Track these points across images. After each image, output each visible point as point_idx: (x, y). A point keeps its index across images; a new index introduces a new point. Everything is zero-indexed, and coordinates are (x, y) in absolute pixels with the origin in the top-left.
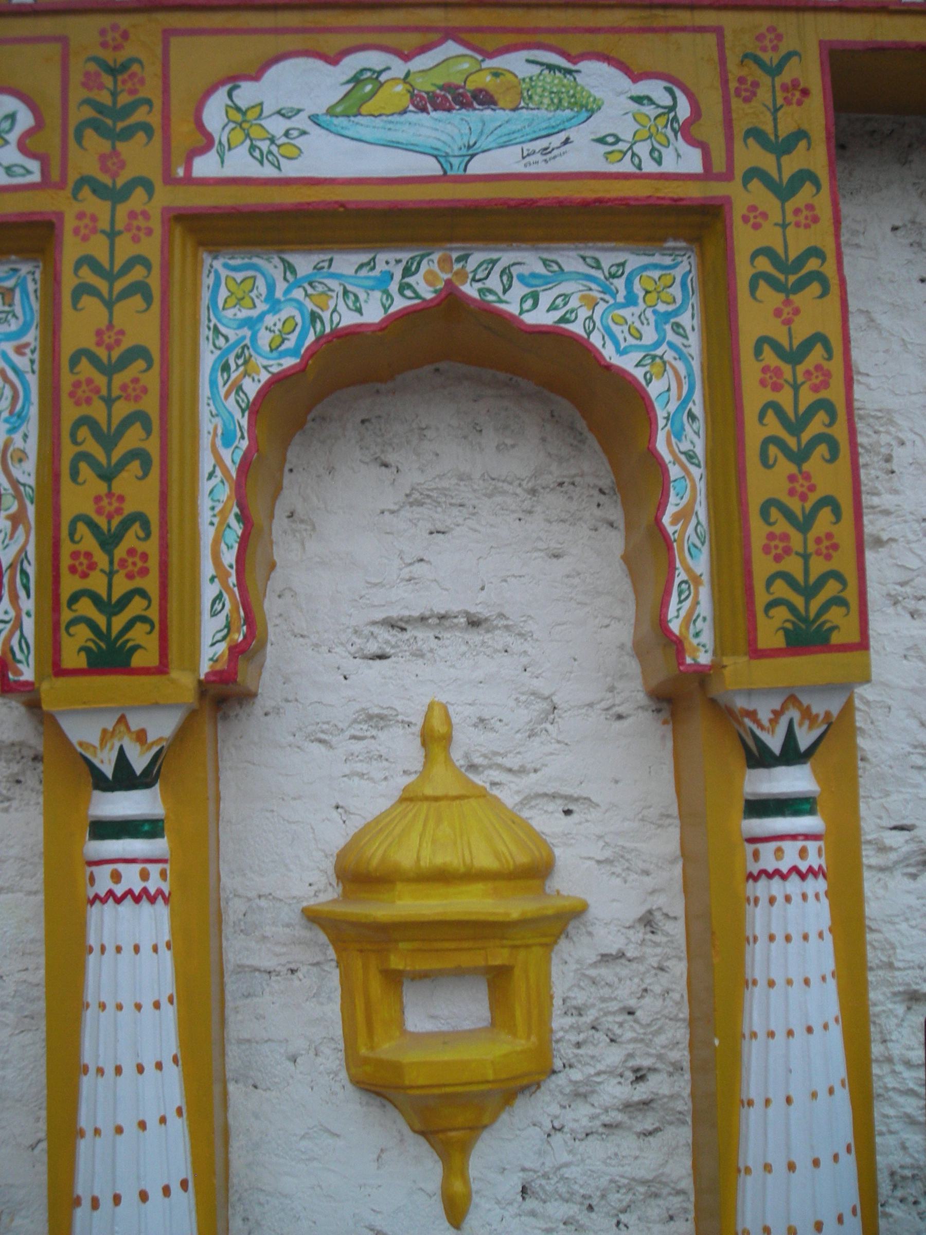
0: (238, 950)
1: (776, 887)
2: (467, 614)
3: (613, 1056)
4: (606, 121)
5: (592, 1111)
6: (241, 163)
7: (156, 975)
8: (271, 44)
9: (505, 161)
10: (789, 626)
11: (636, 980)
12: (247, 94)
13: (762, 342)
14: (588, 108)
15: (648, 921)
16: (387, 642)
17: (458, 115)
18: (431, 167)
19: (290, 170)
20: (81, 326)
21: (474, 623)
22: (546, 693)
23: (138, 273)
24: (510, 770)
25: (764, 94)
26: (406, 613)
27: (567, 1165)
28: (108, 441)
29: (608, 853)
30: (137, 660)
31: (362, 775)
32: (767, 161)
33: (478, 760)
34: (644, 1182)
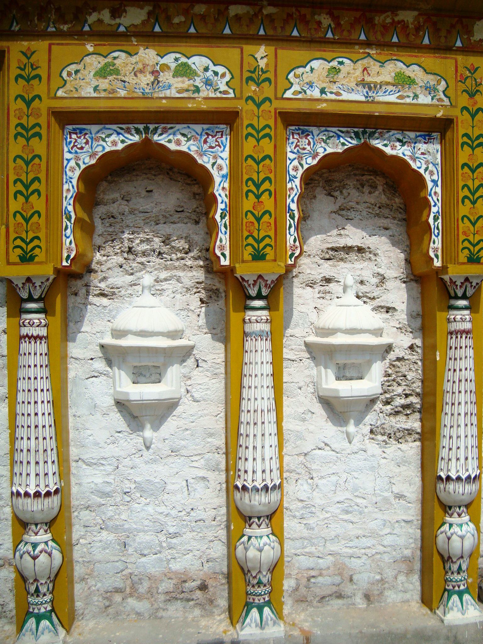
2: (358, 247)
3: (400, 390)
5: (392, 407)
10: (468, 256)
11: (407, 366)
13: (465, 164)
15: (411, 347)
16: (332, 255)
20: (249, 147)
21: (360, 250)
22: (382, 273)
23: (267, 131)
24: (370, 298)
26: (338, 245)
27: (384, 424)
28: (258, 186)
29: (401, 326)
30: (268, 257)
31: (323, 298)
33: (361, 294)
34: (407, 430)
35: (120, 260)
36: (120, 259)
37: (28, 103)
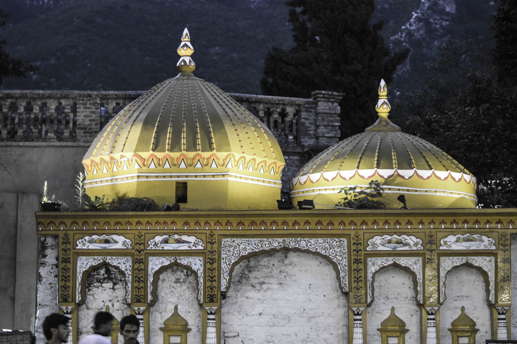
0: (441, 334)
1: (501, 328)
4: (485, 243)
6: (445, 248)
7: (434, 335)
8: (448, 233)
9: (474, 248)
12: (446, 239)
14: (483, 241)
15: (486, 332)
17: (469, 242)
18: (465, 248)
19: (450, 249)
21: (467, 297)
25: (503, 240)
32: (503, 248)
35: (383, 301)
36: (383, 301)
37: (357, 252)
